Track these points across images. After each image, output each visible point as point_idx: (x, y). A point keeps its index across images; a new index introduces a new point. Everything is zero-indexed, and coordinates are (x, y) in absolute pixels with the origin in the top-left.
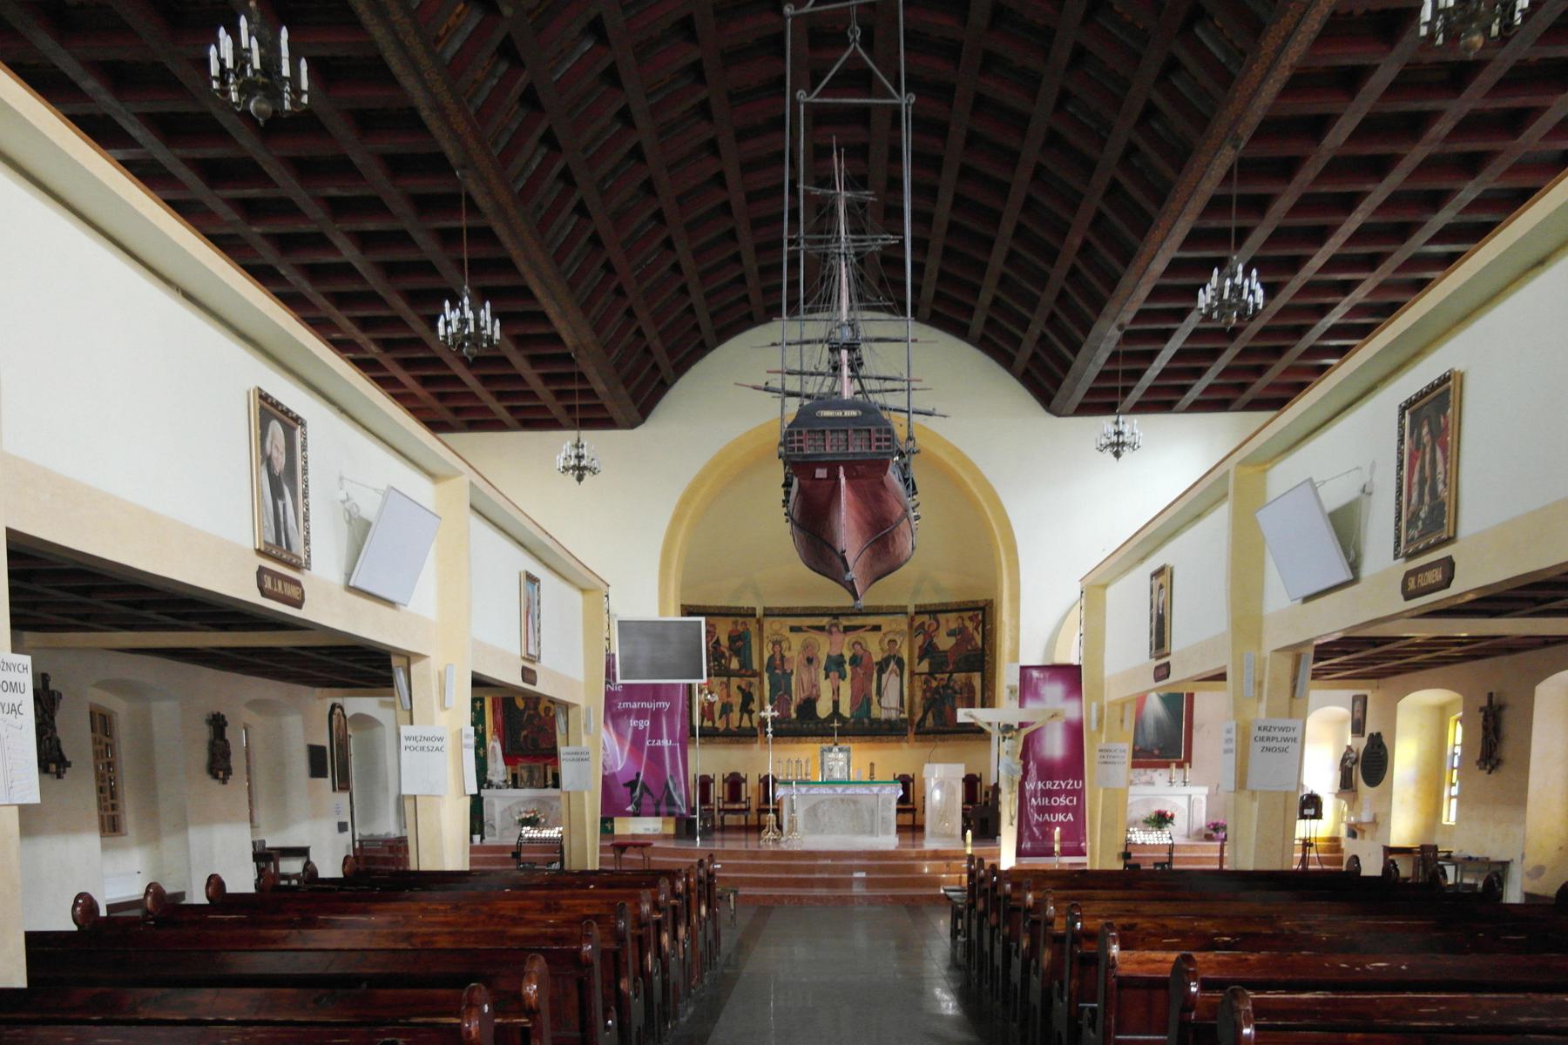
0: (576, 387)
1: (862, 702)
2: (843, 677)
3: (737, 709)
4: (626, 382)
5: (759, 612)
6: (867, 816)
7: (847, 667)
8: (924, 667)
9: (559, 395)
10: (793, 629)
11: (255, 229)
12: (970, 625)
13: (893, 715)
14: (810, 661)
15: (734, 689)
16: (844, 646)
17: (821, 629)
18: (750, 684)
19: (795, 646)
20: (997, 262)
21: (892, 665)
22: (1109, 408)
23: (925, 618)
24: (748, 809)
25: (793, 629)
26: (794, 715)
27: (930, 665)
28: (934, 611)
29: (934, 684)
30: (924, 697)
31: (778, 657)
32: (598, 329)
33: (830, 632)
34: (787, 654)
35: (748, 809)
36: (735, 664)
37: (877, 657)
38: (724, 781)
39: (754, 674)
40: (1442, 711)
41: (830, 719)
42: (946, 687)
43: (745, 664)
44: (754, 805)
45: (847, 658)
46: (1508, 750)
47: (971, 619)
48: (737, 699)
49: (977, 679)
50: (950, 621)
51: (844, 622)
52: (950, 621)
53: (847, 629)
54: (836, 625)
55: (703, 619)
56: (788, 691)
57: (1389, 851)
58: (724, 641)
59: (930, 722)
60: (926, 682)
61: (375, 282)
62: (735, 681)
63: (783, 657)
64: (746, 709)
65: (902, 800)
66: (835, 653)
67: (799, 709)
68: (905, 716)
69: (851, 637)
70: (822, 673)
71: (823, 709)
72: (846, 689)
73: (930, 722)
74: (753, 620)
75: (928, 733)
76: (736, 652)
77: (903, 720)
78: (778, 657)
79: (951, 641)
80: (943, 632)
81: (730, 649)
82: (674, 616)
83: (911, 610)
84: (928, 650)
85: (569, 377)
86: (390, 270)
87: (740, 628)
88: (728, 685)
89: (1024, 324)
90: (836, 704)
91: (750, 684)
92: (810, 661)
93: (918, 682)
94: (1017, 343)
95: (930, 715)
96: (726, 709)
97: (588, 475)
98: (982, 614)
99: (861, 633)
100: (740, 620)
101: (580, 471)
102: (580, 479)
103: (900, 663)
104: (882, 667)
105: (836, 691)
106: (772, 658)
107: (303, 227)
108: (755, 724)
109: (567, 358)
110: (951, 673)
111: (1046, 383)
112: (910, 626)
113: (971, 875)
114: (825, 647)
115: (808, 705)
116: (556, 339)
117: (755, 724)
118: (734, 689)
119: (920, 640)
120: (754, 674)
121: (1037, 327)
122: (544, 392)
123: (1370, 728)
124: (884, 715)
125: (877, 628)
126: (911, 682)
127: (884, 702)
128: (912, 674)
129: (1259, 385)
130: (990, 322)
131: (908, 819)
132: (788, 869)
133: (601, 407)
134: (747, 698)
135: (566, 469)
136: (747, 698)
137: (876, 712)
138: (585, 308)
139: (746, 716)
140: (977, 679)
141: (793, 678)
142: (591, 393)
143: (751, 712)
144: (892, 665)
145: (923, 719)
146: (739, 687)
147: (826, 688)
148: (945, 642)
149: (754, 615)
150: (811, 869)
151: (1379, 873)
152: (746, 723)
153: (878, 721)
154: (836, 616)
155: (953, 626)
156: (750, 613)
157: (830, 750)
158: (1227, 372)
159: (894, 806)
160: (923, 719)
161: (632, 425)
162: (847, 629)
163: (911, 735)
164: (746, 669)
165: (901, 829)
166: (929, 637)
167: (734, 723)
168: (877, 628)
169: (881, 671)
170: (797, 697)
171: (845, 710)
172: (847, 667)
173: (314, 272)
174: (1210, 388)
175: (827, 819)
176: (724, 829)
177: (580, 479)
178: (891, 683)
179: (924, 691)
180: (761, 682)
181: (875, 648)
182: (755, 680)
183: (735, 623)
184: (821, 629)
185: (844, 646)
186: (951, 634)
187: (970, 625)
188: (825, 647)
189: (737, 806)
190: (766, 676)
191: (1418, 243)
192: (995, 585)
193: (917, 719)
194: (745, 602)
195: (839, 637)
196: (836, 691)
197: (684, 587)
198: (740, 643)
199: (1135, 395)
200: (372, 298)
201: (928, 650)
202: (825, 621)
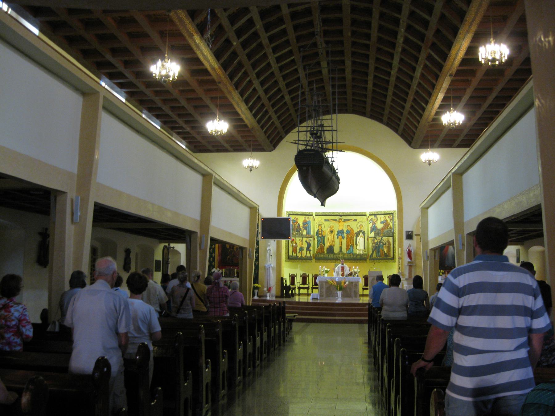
2: (343, 238)
3: (305, 249)
7: (345, 235)
8: (372, 235)
10: (326, 220)
12: (389, 220)
13: (361, 252)
17: (336, 220)
18: (310, 240)
21: (361, 234)
23: (373, 217)
25: (326, 220)
26: (326, 252)
27: (375, 234)
29: (376, 241)
30: (372, 246)
31: (320, 230)
33: (339, 222)
34: (323, 229)
35: (308, 288)
36: (305, 233)
37: (356, 231)
38: (301, 276)
41: (339, 254)
42: (380, 242)
44: (311, 286)
45: (345, 231)
47: (389, 217)
48: (305, 246)
50: (381, 218)
51: (344, 218)
52: (381, 218)
53: (345, 220)
54: (341, 219)
56: (324, 244)
59: (374, 255)
60: (373, 240)
62: (305, 239)
63: (322, 230)
64: (308, 249)
66: (340, 229)
67: (328, 249)
68: (366, 253)
69: (347, 223)
70: (336, 236)
71: (336, 250)
72: (344, 241)
73: (374, 255)
75: (374, 259)
76: (305, 228)
77: (366, 254)
78: (320, 230)
80: (379, 221)
81: (303, 227)
83: (368, 215)
87: (307, 220)
88: (302, 241)
90: (341, 248)
91: (310, 240)
92: (332, 232)
95: (375, 253)
100: (307, 217)
103: (364, 233)
104: (358, 234)
108: (312, 255)
110: (382, 237)
112: (367, 220)
114: (337, 227)
117: (312, 255)
119: (371, 225)
124: (358, 252)
125: (355, 220)
126: (368, 240)
127: (358, 248)
128: (368, 237)
136: (309, 245)
137: (355, 252)
139: (308, 252)
141: (325, 238)
143: (310, 251)
147: (337, 242)
148: (379, 226)
149: (312, 215)
152: (308, 255)
153: (357, 255)
155: (383, 219)
160: (372, 254)
161: (271, 151)
162: (345, 220)
163: (368, 260)
166: (374, 223)
168: (355, 220)
169: (357, 236)
170: (327, 245)
178: (360, 240)
179: (373, 244)
180: (314, 239)
182: (312, 239)
184: (336, 220)
186: (382, 223)
190: (316, 237)
193: (370, 254)
195: (342, 224)
201: (374, 229)
202: (337, 218)
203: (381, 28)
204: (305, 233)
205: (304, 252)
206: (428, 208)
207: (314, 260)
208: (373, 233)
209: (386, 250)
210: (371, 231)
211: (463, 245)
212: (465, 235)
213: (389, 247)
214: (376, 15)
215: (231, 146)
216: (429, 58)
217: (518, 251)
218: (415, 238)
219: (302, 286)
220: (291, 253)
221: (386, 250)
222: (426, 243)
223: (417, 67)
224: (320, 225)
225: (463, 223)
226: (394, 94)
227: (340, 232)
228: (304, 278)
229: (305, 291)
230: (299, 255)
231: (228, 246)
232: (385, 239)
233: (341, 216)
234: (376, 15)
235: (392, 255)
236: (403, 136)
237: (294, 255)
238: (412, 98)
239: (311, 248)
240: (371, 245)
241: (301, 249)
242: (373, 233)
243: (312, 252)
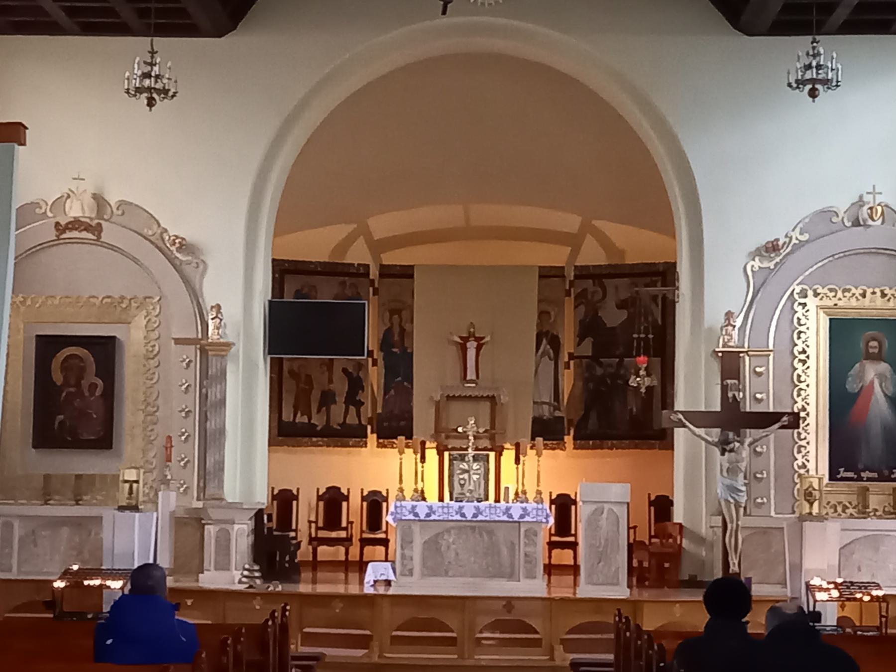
3: (341, 399)
5: (374, 273)
6: (505, 551)
8: (587, 348)
15: (338, 373)
24: (348, 540)
29: (599, 371)
31: (396, 330)
35: (348, 540)
48: (340, 387)
59: (593, 423)
60: (589, 368)
63: (403, 331)
73: (593, 423)
78: (396, 330)
79: (623, 315)
80: (611, 303)
83: (571, 274)
84: (590, 327)
106: (388, 333)
110: (621, 358)
118: (338, 373)
134: (356, 384)
139: (352, 409)
143: (359, 404)
146: (345, 371)
148: (613, 317)
152: (352, 419)
155: (624, 295)
156: (362, 272)
161: (219, 32)
163: (569, 439)
175: (452, 555)
183: (343, 283)
186: (621, 305)
189: (334, 535)
207: (372, 438)
208: (588, 343)
215: (71, 12)
219: (323, 534)
228: (333, 500)
230: (318, 420)
237: (302, 419)
239: (366, 397)
241: (327, 399)
242: (588, 343)
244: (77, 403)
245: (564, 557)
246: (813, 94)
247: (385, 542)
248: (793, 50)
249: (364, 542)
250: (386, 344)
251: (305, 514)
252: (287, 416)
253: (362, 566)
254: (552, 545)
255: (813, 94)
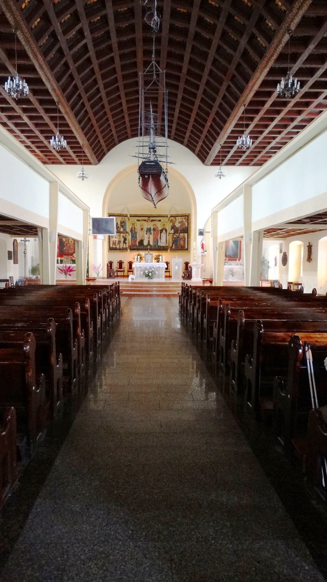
0: (82, 154)
1: (156, 240)
2: (151, 234)
4: (95, 153)
5: (129, 216)
7: (152, 231)
8: (172, 231)
9: (77, 156)
11: (3, 114)
12: (184, 220)
13: (164, 245)
14: (142, 229)
15: (121, 236)
16: (151, 225)
17: (145, 220)
19: (138, 225)
20: (190, 127)
21: (164, 231)
22: (219, 164)
24: (124, 271)
25: (138, 220)
28: (175, 216)
29: (175, 236)
32: (88, 140)
35: (124, 271)
36: (122, 230)
37: (160, 229)
39: (127, 233)
40: (300, 246)
41: (147, 246)
42: (178, 237)
43: (125, 230)
46: (313, 257)
48: (122, 240)
49: (186, 235)
51: (151, 219)
53: (152, 221)
55: (115, 218)
56: (136, 238)
57: (289, 283)
58: (119, 224)
59: (174, 247)
61: (32, 127)
62: (122, 235)
64: (124, 242)
65: (167, 269)
67: (139, 242)
69: (153, 223)
71: (145, 243)
72: (152, 237)
73: (174, 247)
74: (126, 218)
76: (122, 226)
79: (180, 225)
80: (177, 222)
82: (106, 217)
84: (173, 227)
85: (81, 152)
86: (37, 125)
88: (120, 236)
89: (197, 142)
90: (149, 241)
92: (142, 229)
93: (171, 236)
94: (196, 147)
96: (119, 242)
97: (85, 179)
98: (187, 217)
99: (155, 222)
101: (83, 178)
102: (83, 180)
103: (166, 230)
104: (161, 231)
105: (149, 238)
106: (132, 228)
107: (15, 114)
109: (80, 147)
111: (203, 156)
113: (182, 287)
115: (141, 242)
116: (78, 143)
118: (121, 236)
120: (127, 233)
121: (200, 143)
122: (74, 156)
123: (283, 251)
124: (162, 245)
125: (160, 221)
128: (169, 233)
129: (256, 160)
130: (189, 141)
131: (168, 274)
132: (136, 287)
133: (88, 160)
134: (125, 239)
135: (79, 177)
136: (125, 239)
137: (159, 244)
138: (86, 134)
140: (186, 235)
142: (86, 156)
143: (126, 243)
144: (164, 231)
145: (172, 246)
148: (178, 225)
150: (142, 287)
151: (287, 288)
152: (125, 246)
154: (149, 217)
155: (180, 220)
157: (147, 254)
158: (247, 157)
159: (164, 270)
160: (172, 246)
162: (152, 221)
163: (169, 250)
164: (125, 232)
165: (166, 277)
166: (174, 223)
167: (121, 247)
168: (160, 221)
169: (161, 233)
170: (138, 239)
171: (151, 243)
172: (152, 231)
173: (16, 125)
174: (244, 160)
176: (117, 276)
177: (83, 180)
178: (163, 235)
181: (159, 226)
184: (145, 220)
185: (151, 225)
186: (179, 223)
187: (184, 220)
188: (146, 225)
190: (130, 233)
191: (289, 129)
192: (191, 210)
193: (171, 246)
194: (125, 213)
196: (149, 238)
197: (109, 209)
198: (123, 224)
199: (225, 161)
200: (31, 131)
203: (192, 62)
204: (122, 230)
205: (122, 244)
206: (217, 212)
207: (129, 250)
208: (173, 230)
209: (182, 243)
210: (172, 229)
211: (251, 239)
212: (252, 232)
213: (184, 241)
214: (189, 48)
216: (228, 88)
217: (281, 245)
218: (205, 234)
220: (111, 246)
221: (182, 243)
222: (215, 239)
223: (218, 98)
224: (133, 224)
225: (251, 223)
226: (195, 120)
227: (149, 230)
228: (121, 263)
229: (122, 274)
230: (118, 247)
231: (64, 240)
232: (182, 234)
233: (149, 217)
234: (189, 48)
235: (186, 247)
236: (198, 156)
238: (209, 124)
239: (127, 242)
240: (171, 239)
242: (173, 230)
243: (127, 245)
244: (68, 245)
245: (168, 274)
246: (220, 178)
247: (132, 271)
248: (216, 169)
249: (128, 271)
250: (131, 231)
251: (115, 266)
252: (111, 246)
253: (128, 276)
254: (166, 272)
255: (220, 178)
